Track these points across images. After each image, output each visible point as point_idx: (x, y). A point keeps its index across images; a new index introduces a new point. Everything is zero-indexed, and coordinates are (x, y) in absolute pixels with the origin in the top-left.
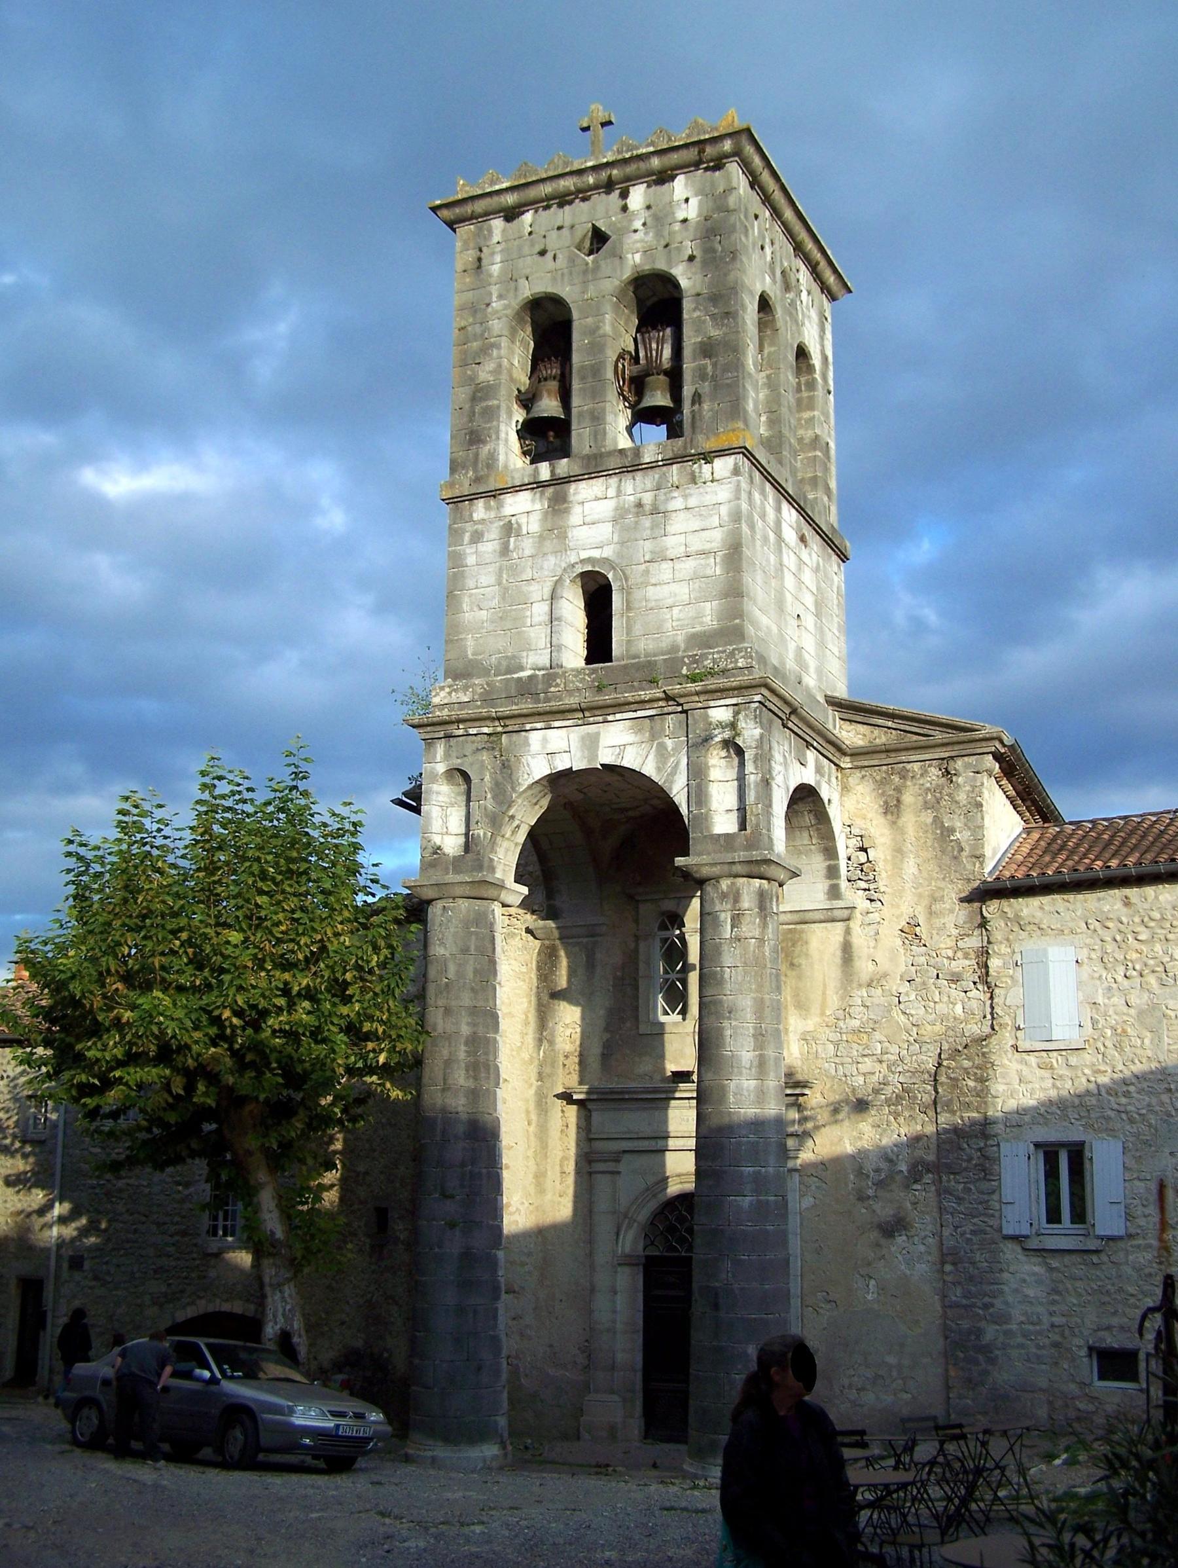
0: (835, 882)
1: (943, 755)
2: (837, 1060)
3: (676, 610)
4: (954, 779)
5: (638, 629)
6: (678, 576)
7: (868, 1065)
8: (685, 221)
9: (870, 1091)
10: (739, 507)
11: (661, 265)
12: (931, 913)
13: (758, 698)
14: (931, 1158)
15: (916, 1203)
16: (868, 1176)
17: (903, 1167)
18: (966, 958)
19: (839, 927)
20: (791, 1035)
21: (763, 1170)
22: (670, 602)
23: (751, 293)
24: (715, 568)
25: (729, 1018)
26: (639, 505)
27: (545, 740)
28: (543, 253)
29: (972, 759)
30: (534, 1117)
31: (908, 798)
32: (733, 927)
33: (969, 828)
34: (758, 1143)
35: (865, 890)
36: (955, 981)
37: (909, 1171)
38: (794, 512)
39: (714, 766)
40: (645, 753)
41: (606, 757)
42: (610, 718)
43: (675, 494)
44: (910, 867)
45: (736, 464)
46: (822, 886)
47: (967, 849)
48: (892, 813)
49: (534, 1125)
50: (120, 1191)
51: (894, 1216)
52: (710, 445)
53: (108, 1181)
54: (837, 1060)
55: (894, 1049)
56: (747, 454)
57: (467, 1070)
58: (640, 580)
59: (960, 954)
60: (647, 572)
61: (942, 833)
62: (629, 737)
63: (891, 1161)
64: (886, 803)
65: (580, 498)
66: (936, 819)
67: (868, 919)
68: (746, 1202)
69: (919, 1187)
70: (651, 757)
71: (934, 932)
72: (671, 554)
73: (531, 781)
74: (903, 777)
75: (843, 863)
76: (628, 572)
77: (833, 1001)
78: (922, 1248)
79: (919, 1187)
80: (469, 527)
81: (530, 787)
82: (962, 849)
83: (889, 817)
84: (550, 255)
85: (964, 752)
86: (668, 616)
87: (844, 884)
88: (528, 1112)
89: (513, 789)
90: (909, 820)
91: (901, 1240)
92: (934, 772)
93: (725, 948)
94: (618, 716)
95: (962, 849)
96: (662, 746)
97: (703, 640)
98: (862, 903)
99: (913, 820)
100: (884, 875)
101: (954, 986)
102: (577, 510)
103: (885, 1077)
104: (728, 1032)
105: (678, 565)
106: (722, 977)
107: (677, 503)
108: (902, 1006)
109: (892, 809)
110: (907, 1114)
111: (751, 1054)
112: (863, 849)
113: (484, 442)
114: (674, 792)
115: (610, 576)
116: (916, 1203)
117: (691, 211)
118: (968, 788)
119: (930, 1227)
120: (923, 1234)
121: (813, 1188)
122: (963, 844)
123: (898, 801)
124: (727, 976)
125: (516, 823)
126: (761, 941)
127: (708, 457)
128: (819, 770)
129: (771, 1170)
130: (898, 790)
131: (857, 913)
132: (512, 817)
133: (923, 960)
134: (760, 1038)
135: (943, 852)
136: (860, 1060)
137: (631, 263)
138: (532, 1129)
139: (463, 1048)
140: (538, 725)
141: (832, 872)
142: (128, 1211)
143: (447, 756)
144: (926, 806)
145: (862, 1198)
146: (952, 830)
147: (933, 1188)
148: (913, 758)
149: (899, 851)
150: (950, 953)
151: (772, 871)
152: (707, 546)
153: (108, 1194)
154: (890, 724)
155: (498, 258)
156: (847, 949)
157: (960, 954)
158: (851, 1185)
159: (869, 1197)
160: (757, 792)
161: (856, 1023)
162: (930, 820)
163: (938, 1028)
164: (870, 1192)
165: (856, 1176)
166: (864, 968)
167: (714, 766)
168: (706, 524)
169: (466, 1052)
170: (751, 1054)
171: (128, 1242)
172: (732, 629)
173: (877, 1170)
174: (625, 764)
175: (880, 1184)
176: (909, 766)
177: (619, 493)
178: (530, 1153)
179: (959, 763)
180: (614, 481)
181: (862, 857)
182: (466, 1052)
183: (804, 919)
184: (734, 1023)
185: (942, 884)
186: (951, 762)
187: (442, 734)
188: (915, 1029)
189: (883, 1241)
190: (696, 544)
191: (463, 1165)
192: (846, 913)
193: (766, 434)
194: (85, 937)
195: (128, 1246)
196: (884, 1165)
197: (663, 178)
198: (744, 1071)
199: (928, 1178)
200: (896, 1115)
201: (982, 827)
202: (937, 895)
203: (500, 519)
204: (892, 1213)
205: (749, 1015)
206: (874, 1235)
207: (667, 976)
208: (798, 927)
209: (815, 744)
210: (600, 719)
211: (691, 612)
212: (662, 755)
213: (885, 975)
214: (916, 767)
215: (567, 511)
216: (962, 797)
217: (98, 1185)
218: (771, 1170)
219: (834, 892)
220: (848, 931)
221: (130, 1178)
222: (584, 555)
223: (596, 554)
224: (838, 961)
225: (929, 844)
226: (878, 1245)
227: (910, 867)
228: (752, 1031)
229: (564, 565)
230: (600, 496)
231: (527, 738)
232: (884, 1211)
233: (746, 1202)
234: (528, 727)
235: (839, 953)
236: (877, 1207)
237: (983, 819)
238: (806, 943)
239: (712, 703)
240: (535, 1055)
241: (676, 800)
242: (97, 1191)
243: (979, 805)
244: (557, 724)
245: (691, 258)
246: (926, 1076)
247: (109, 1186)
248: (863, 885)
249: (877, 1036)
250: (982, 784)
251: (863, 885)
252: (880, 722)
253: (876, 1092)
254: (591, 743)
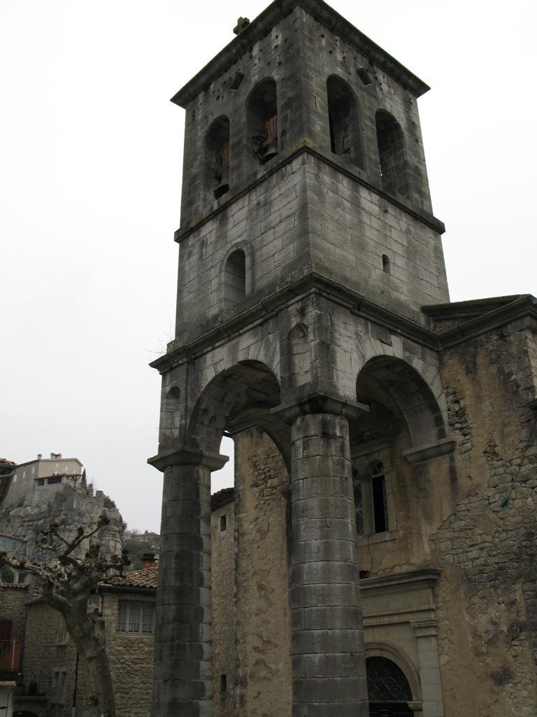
0: (441, 427)
1: (497, 325)
2: (453, 552)
3: (276, 256)
4: (507, 339)
5: (258, 275)
6: (277, 235)
7: (474, 553)
8: (276, 47)
9: (477, 572)
10: (305, 181)
11: (266, 75)
12: (504, 436)
13: (313, 290)
14: (523, 618)
15: (516, 656)
16: (481, 636)
17: (505, 628)
18: (531, 463)
19: (447, 458)
20: (424, 538)
21: (330, 632)
22: (273, 252)
23: (320, 73)
24: (294, 222)
25: (303, 517)
26: (259, 204)
27: (213, 356)
28: (218, 98)
29: (518, 323)
30: (288, 611)
31: (481, 360)
32: (304, 449)
33: (521, 370)
34: (325, 610)
35: (461, 429)
36: (525, 482)
37: (508, 631)
38: (375, 197)
39: (296, 344)
40: (258, 348)
41: (241, 357)
42: (241, 331)
43: (275, 190)
44: (486, 406)
45: (303, 159)
46: (434, 432)
47: (522, 385)
48: (471, 372)
49: (289, 615)
50: (136, 671)
51: (502, 667)
52: (287, 153)
53: (128, 665)
54: (453, 552)
55: (489, 538)
56: (311, 152)
57: (176, 575)
58: (259, 246)
59: (526, 461)
60: (262, 239)
61: (504, 378)
62: (251, 341)
63: (495, 624)
64: (467, 367)
65: (232, 213)
66: (501, 371)
67: (463, 449)
68: (317, 658)
69: (517, 643)
70: (262, 349)
71: (507, 448)
72: (273, 225)
73: (207, 383)
74: (476, 347)
75: (445, 416)
76: (254, 244)
77: (447, 510)
78: (525, 693)
79: (517, 643)
80: (187, 251)
81: (208, 386)
82: (518, 386)
83: (470, 375)
84: (221, 98)
85: (511, 319)
86: (272, 261)
87: (447, 428)
88: (285, 609)
89: (199, 391)
90: (482, 374)
91: (509, 687)
92: (495, 337)
93: (300, 465)
94: (245, 329)
95: (518, 386)
96: (268, 340)
97: (291, 267)
98: (458, 437)
99: (486, 373)
100: (471, 416)
101: (524, 485)
102: (231, 220)
103: (485, 560)
104: (302, 527)
105: (276, 230)
106: (299, 487)
107: (276, 195)
108: (492, 506)
109: (471, 370)
110: (503, 586)
111: (318, 542)
112: (457, 402)
113: (194, 204)
114: (274, 367)
115: (244, 249)
116: (516, 656)
117: (279, 41)
118: (517, 343)
119: (529, 675)
120: (524, 681)
121: (446, 648)
122: (519, 382)
123: (475, 363)
124: (301, 485)
125: (210, 415)
126: (325, 456)
127: (289, 161)
128: (406, 349)
129: (338, 631)
130: (474, 356)
131: (458, 447)
132: (205, 411)
133: (501, 470)
134: (326, 529)
135: (506, 390)
136: (468, 550)
137: (254, 81)
138: (287, 619)
139: (174, 561)
140: (209, 348)
141: (439, 421)
142: (142, 682)
143: (171, 380)
144: (492, 362)
145: (478, 654)
146: (511, 374)
147: (527, 644)
148: (480, 332)
149: (479, 398)
150: (519, 461)
151: (329, 406)
152: (291, 211)
153: (128, 672)
154: (463, 315)
155: (201, 112)
156: (453, 472)
157: (526, 461)
158: (470, 645)
159: (483, 653)
160: (316, 352)
161: (463, 523)
162: (495, 371)
163: (519, 519)
164: (484, 649)
165: (473, 637)
166: (464, 483)
167: (296, 344)
168: (290, 199)
169: (176, 563)
170: (318, 542)
171: (143, 700)
172: (304, 255)
173: (487, 632)
174: (250, 358)
175: (490, 642)
176: (478, 339)
177: (249, 200)
178: (287, 636)
179: (509, 327)
180: (246, 197)
181: (457, 407)
182: (176, 563)
183: (424, 457)
184: (306, 520)
185: (507, 413)
186: (504, 329)
187: (168, 369)
188: (502, 521)
189: (497, 689)
190: (285, 213)
191: (172, 640)
192: (448, 447)
193: (354, 156)
194: (267, 555)
195: (142, 702)
196: (491, 628)
197: (267, 32)
198: (313, 555)
199: (523, 636)
200: (495, 587)
201: (530, 367)
202: (506, 421)
203: (199, 240)
204: (500, 665)
205: (316, 512)
206: (490, 683)
207: (361, 509)
208: (422, 463)
209: (399, 331)
210: (237, 334)
211: (283, 254)
212: (267, 347)
213: (478, 485)
214: (482, 338)
215: (227, 223)
216: (514, 350)
217: (122, 668)
218: (338, 631)
219: (442, 434)
220: (452, 460)
221: (142, 664)
222: (234, 243)
223: (239, 240)
224: (449, 481)
225: (497, 387)
226: (492, 691)
227: (486, 406)
228: (318, 524)
229: (225, 253)
230: (241, 207)
231: (205, 358)
232: (495, 664)
233: (317, 658)
234: (205, 351)
235: (448, 476)
236: (489, 660)
237: (530, 361)
238: (428, 472)
239: (290, 303)
240: (287, 572)
241: (275, 372)
242: (121, 671)
243: (526, 352)
244: (217, 345)
245: (280, 63)
246: (513, 556)
247: (129, 668)
248: (458, 425)
249: (478, 531)
250: (526, 337)
251: (458, 425)
252: (457, 315)
253: (481, 572)
254: (233, 352)
